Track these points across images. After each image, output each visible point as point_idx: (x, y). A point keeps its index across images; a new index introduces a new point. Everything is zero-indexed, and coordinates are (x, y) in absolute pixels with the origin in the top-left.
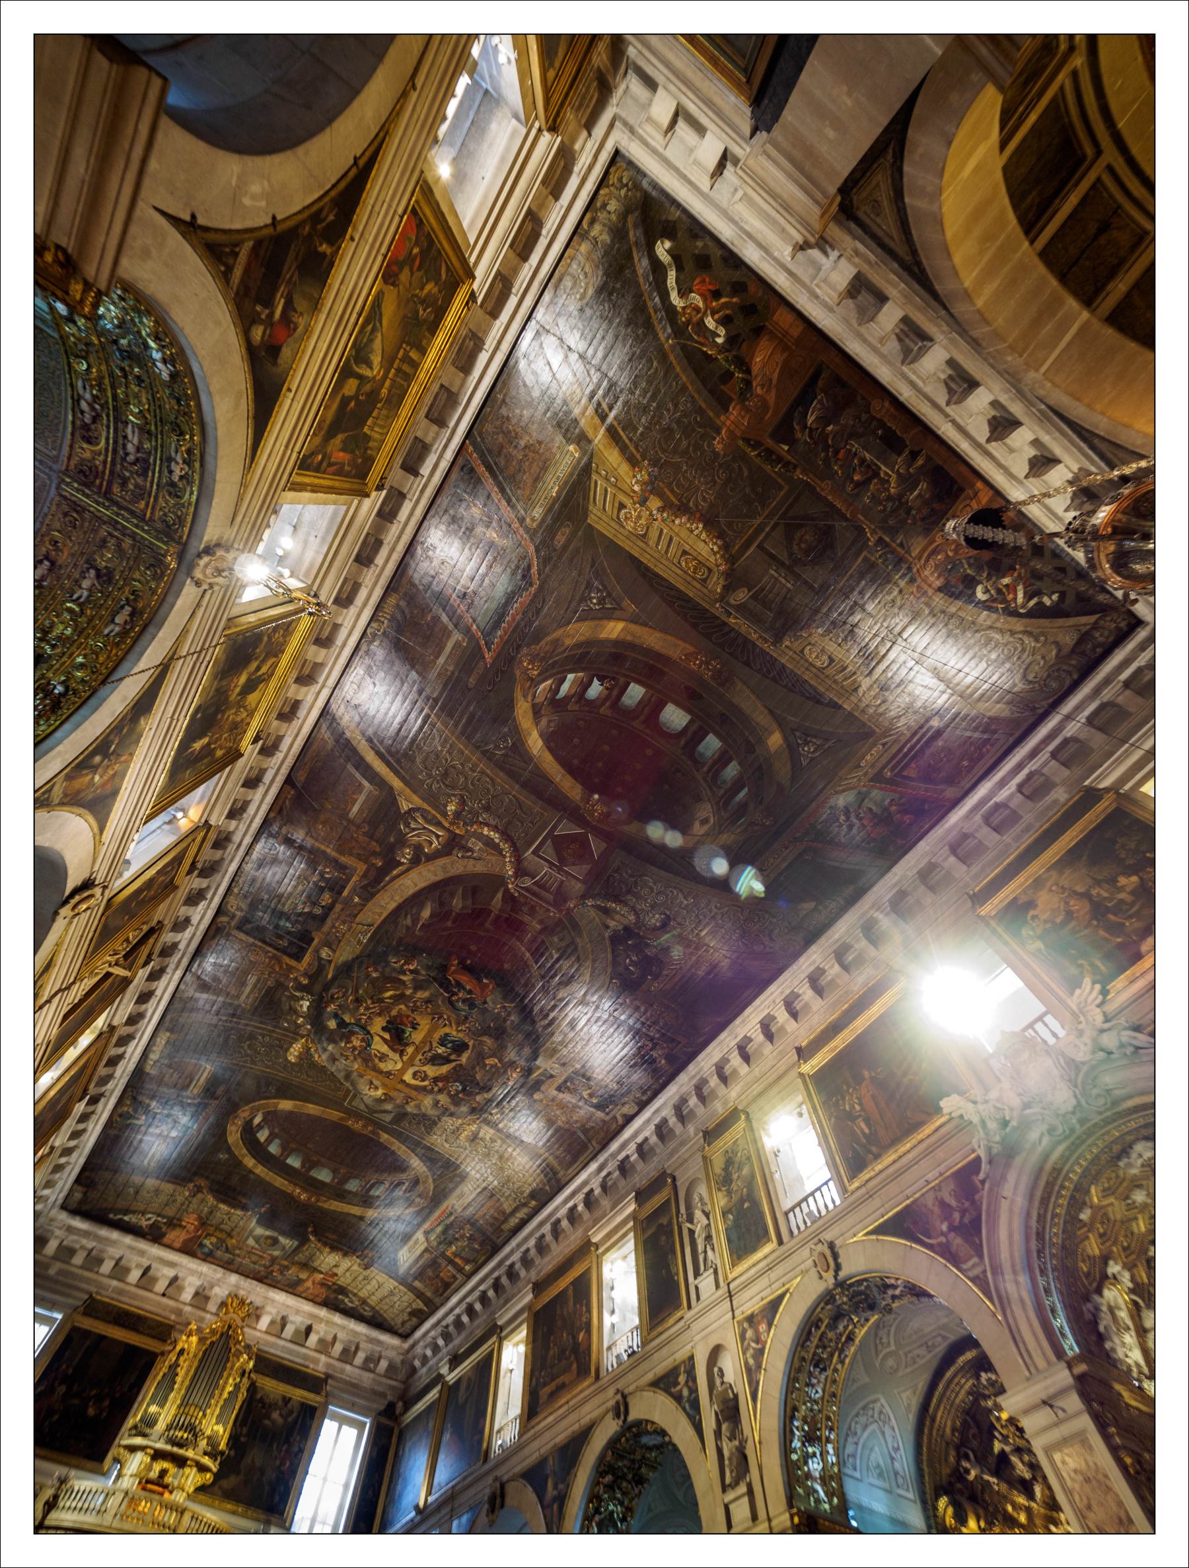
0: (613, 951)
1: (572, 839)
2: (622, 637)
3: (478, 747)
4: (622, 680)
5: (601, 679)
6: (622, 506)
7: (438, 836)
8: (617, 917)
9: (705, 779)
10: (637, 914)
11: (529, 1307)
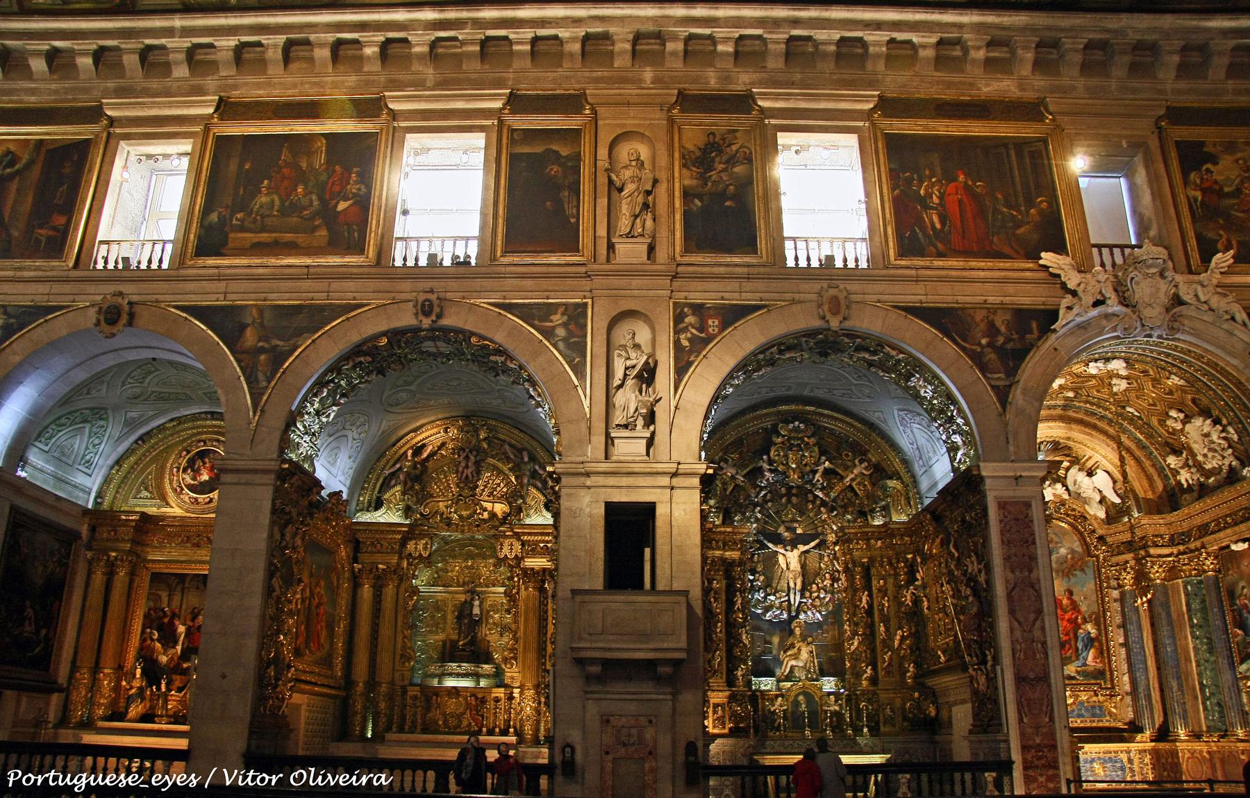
11: (206, 121)
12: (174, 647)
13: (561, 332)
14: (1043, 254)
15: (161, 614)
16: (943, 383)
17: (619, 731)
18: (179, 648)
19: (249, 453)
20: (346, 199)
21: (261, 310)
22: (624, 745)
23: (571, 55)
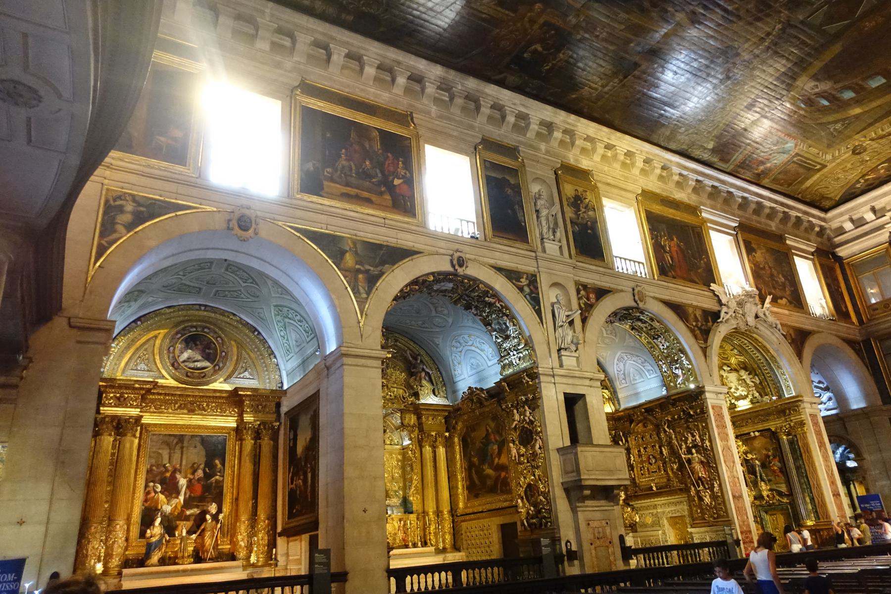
12: (177, 498)
13: (527, 289)
14: (712, 284)
15: (162, 469)
16: (679, 342)
17: (594, 530)
18: (182, 498)
19: (360, 342)
20: (399, 178)
21: (355, 243)
22: (598, 538)
23: (508, 123)
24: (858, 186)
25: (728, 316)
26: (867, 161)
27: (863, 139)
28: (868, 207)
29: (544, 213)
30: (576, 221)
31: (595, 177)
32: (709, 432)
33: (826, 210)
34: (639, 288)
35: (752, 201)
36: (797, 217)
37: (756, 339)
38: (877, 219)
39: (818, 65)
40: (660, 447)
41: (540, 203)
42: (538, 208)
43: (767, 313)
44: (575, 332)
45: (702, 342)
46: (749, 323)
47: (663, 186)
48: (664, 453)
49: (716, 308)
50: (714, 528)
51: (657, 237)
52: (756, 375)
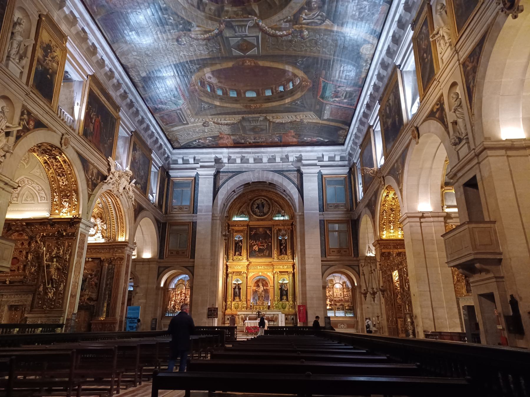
0: (182, 19)
1: (248, 50)
2: (284, 100)
3: (309, 57)
4: (275, 94)
5: (281, 92)
6: (306, 117)
7: (304, 19)
8: (199, 33)
9: (225, 88)
10: (194, 38)
14: (110, 157)
24: (194, 143)
25: (111, 181)
26: (205, 132)
27: (211, 120)
28: (193, 156)
29: (19, 38)
30: (42, 62)
31: (67, 43)
32: (72, 250)
33: (174, 148)
34: (67, 136)
35: (146, 123)
36: (161, 144)
37: (117, 202)
38: (194, 164)
39: (218, 67)
40: (27, 253)
41: (18, 28)
42: (14, 31)
43: (131, 188)
44: (8, 141)
45: (91, 190)
46: (119, 190)
47: (106, 81)
48: (29, 258)
49: (106, 173)
50: (48, 315)
51: (90, 109)
52: (105, 223)
